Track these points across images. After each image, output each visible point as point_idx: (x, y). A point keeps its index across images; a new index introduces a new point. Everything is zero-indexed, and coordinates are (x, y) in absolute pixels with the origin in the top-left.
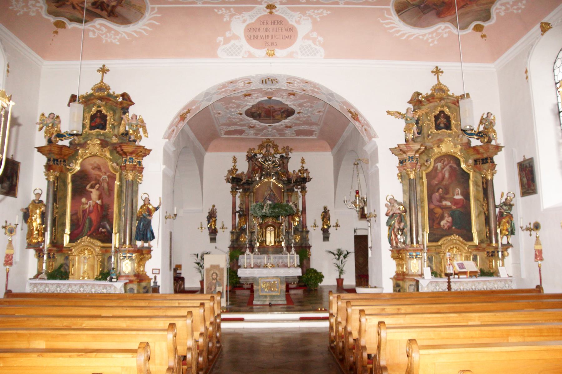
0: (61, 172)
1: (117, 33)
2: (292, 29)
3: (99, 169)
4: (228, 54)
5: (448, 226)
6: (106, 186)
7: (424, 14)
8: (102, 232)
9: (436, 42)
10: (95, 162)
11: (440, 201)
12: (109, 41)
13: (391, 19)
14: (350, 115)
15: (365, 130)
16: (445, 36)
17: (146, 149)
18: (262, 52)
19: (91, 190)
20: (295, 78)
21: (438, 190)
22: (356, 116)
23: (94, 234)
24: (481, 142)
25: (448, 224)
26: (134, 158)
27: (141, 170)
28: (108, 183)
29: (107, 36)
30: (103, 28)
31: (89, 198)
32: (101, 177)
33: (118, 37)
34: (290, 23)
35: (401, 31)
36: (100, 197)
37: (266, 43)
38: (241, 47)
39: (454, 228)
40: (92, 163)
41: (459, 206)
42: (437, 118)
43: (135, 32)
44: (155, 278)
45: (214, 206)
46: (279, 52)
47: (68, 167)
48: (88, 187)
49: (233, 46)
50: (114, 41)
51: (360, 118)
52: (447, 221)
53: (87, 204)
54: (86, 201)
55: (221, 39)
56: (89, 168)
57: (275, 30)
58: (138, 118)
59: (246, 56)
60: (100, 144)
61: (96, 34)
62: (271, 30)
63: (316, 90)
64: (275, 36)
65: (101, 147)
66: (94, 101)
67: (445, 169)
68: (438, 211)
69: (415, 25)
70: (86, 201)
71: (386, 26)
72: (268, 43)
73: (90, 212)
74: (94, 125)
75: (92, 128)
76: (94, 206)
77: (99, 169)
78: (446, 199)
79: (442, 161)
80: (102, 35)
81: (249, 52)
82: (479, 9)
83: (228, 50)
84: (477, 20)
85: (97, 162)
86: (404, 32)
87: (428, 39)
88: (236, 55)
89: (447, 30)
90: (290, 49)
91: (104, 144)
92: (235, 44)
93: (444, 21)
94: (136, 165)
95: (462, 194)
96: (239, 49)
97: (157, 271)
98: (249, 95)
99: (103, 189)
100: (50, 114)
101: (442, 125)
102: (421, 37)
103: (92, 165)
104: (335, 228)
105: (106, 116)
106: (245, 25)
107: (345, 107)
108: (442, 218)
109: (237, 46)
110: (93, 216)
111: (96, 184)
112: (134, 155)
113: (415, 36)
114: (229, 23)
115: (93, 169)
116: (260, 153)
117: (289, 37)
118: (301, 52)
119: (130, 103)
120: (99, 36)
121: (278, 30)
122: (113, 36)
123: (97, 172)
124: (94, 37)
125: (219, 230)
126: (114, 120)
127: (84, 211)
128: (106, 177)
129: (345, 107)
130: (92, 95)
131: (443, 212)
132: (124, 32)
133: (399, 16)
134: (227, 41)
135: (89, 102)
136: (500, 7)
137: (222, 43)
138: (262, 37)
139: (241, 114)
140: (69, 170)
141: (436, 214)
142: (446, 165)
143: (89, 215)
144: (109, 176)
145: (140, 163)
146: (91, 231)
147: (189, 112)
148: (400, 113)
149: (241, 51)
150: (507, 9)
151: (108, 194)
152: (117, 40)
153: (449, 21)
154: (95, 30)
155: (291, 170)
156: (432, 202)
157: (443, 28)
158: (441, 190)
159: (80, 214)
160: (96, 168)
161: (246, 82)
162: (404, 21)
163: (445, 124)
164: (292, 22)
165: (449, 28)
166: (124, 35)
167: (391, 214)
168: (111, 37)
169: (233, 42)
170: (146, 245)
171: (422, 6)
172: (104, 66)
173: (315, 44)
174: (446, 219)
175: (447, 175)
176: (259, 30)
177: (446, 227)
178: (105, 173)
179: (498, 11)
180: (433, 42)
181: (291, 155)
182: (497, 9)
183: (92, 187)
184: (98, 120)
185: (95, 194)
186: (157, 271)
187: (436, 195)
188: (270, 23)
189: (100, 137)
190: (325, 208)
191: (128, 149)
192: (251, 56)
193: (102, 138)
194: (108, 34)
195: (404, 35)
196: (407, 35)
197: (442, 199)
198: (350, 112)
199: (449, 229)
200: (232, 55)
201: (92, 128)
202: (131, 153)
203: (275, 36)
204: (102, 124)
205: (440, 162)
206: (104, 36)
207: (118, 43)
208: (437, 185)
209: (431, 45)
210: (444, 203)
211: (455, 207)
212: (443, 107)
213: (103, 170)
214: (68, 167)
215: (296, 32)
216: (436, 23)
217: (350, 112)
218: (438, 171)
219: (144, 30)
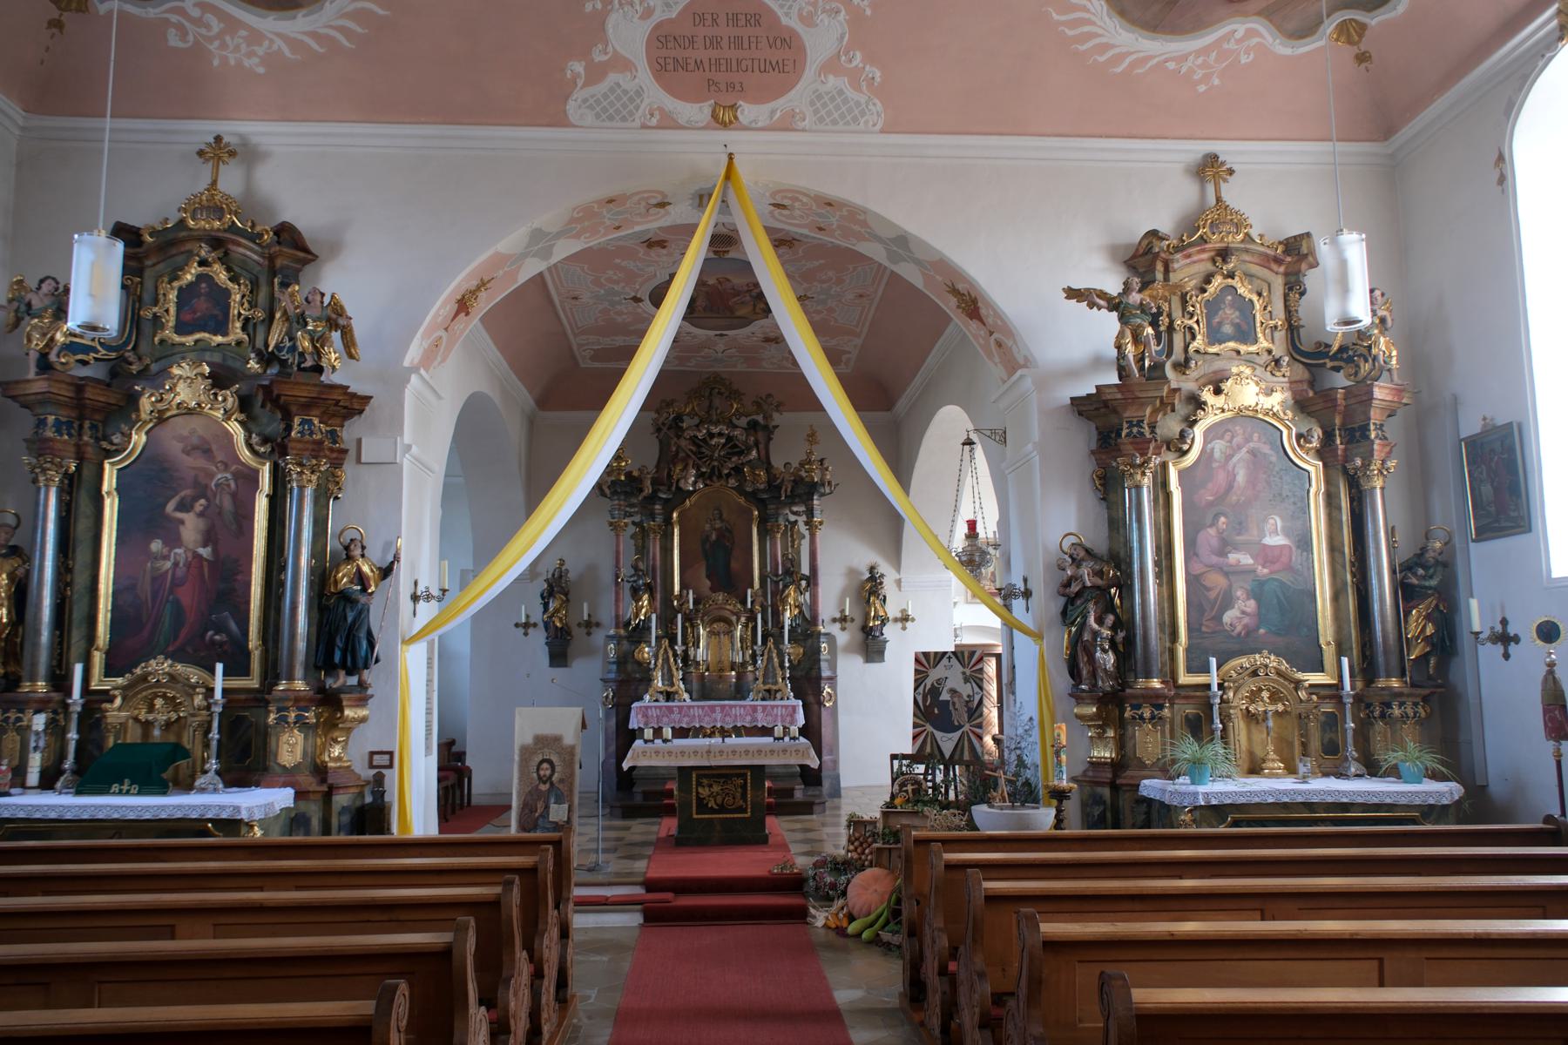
0: (80, 458)
1: (256, 37)
2: (788, 42)
3: (207, 452)
4: (598, 116)
5: (1246, 626)
6: (227, 503)
8: (213, 642)
9: (1216, 82)
10: (193, 431)
11: (1222, 553)
12: (232, 62)
14: (953, 301)
15: (999, 345)
17: (354, 395)
18: (699, 112)
19: (179, 515)
20: (796, 194)
21: (1216, 517)
22: (972, 305)
23: (190, 650)
24: (1348, 376)
25: (1246, 620)
26: (316, 421)
27: (338, 457)
28: (234, 496)
29: (223, 46)
30: (209, 17)
31: (173, 540)
32: (212, 476)
33: (260, 51)
34: (784, 21)
36: (209, 538)
37: (711, 83)
38: (639, 93)
39: (1262, 631)
40: (185, 433)
41: (1277, 567)
42: (1212, 307)
43: (314, 35)
44: (379, 780)
45: (562, 562)
46: (748, 112)
47: (105, 444)
48: (170, 507)
49: (612, 90)
50: (247, 63)
51: (983, 312)
52: (1243, 612)
53: (166, 558)
54: (165, 551)
55: (578, 67)
56: (174, 448)
57: (737, 42)
58: (327, 300)
59: (654, 121)
60: (211, 376)
61: (191, 38)
62: (725, 43)
63: (857, 228)
64: (739, 62)
65: (213, 386)
66: (188, 246)
67: (1235, 459)
68: (1216, 581)
70: (165, 551)
71: (1070, 33)
72: (716, 84)
73: (176, 583)
74: (187, 317)
75: (181, 329)
76: (188, 565)
77: (207, 452)
78: (1237, 548)
79: (1228, 436)
80: (211, 40)
81: (661, 109)
83: (598, 102)
84: (1347, 7)
85: (200, 431)
86: (1124, 50)
87: (1191, 71)
88: (624, 119)
89: (1256, 40)
90: (781, 104)
91: (219, 380)
92: (618, 85)
93: (1245, 14)
94: (320, 443)
95: (1287, 534)
96: (631, 100)
97: (385, 760)
98: (662, 244)
99: (220, 514)
100: (42, 281)
101: (1228, 329)
102: (1171, 65)
103: (181, 439)
104: (899, 625)
105: (227, 293)
106: (646, 27)
107: (939, 278)
108: (1227, 602)
109: (625, 92)
110: (188, 597)
111: (195, 499)
112: (317, 412)
113: (1155, 61)
114: (600, 20)
115: (188, 453)
116: (692, 414)
117: (779, 67)
118: (816, 112)
119: (301, 255)
120: (197, 43)
121: (746, 45)
122: (244, 46)
123: (200, 462)
124: (181, 45)
125: (578, 633)
126: (253, 305)
127: (158, 578)
128: (229, 476)
129: (939, 278)
130: (181, 223)
131: (1230, 586)
132: (278, 35)
134: (596, 73)
135: (174, 251)
137: (580, 83)
138: (699, 65)
139: (637, 300)
140: (109, 454)
141: (1208, 589)
142: (1239, 448)
143: (171, 591)
144: (236, 476)
145: (334, 436)
146: (178, 643)
147: (483, 284)
148: (1102, 295)
149: (637, 108)
151: (234, 527)
152: (256, 60)
153: (1259, 14)
154: (187, 24)
155: (777, 462)
156: (1196, 554)
157: (1238, 35)
158: (1223, 519)
159: (145, 589)
160: (195, 448)
161: (654, 201)
163: (1237, 326)
164: (790, 21)
165: (1260, 35)
166: (279, 43)
167: (1075, 588)
168: (237, 48)
169: (612, 77)
170: (353, 680)
172: (218, 139)
173: (856, 85)
174: (1240, 604)
175: (1241, 477)
176: (692, 41)
177: (1239, 628)
178: (226, 466)
180: (1206, 78)
181: (777, 418)
183: (184, 507)
184: (202, 305)
185: (191, 527)
186: (385, 760)
187: (1209, 536)
188: (722, 20)
189: (208, 356)
190: (872, 569)
191: (299, 391)
192: (668, 122)
193: (217, 358)
194: (228, 38)
195: (1120, 57)
197: (1225, 546)
198: (955, 291)
199: (1248, 634)
200: (611, 118)
201: (181, 329)
202: (307, 406)
203: (739, 62)
204: (216, 316)
205: (1222, 438)
206: (217, 43)
207: (261, 70)
208: (1211, 504)
209: (1202, 88)
210: (1233, 557)
211: (1266, 571)
212: (1231, 275)
213: (220, 456)
214: (105, 444)
215: (802, 49)
216: (1220, 20)
217: (955, 291)
218: (1215, 465)
219: (341, 29)
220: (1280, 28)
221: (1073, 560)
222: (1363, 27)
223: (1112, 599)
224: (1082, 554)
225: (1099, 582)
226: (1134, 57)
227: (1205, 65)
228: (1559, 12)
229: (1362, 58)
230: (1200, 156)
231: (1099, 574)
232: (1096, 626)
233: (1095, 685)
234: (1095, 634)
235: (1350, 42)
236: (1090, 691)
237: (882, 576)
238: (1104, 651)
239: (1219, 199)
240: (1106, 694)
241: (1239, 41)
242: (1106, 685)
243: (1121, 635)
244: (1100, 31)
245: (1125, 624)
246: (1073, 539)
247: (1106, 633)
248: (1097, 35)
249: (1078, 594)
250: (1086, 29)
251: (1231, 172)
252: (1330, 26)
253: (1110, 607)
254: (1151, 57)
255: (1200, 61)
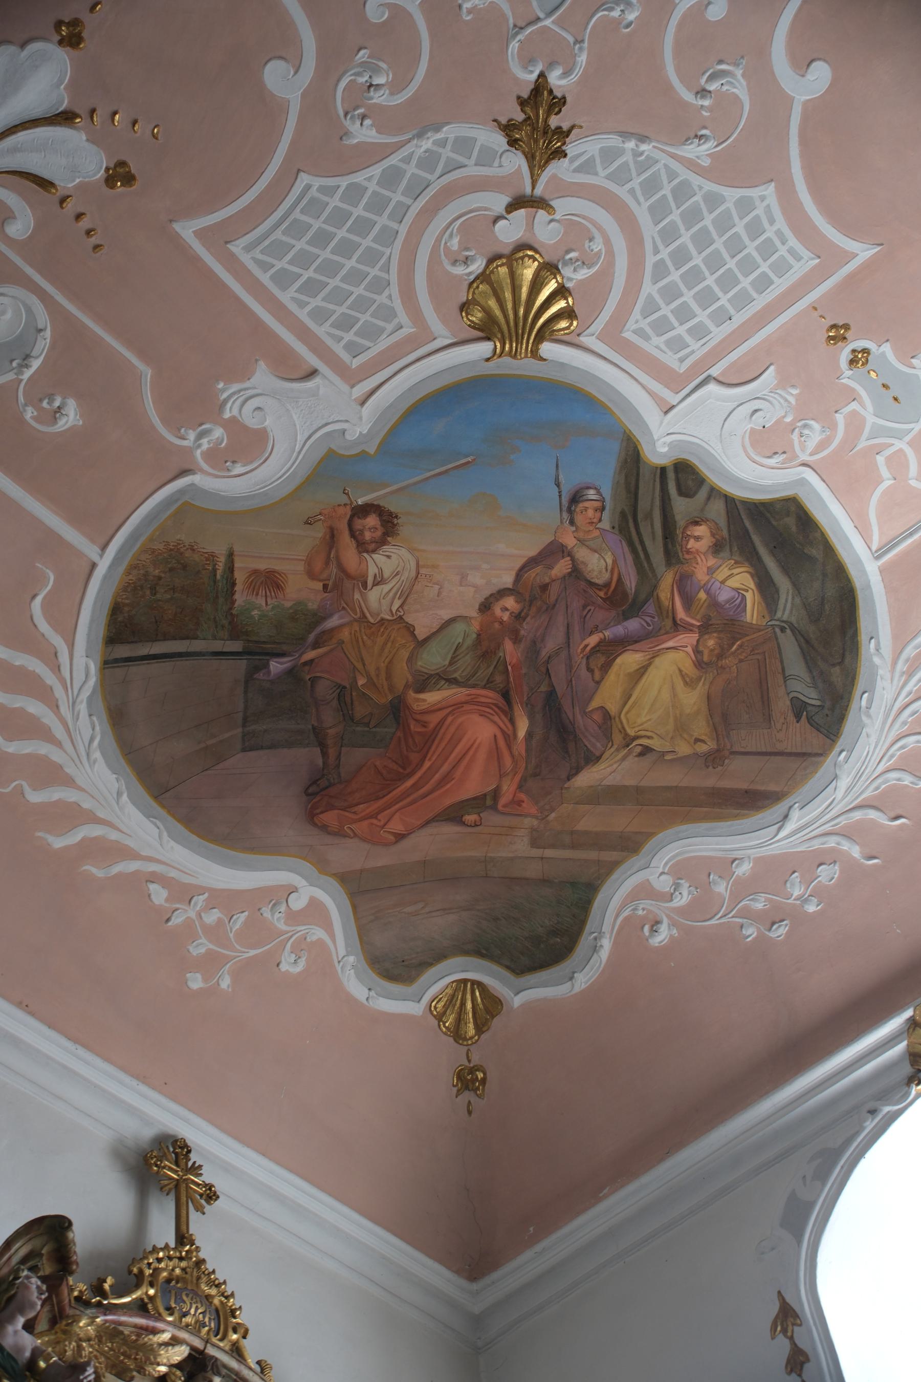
7: (250, 744)
9: (225, 983)
13: (51, 659)
16: (290, 965)
35: (69, 782)
69: (165, 786)
82: (533, 871)
87: (189, 931)
89: (318, 933)
93: (322, 865)
113: (132, 866)
133: (107, 664)
136: (664, 883)
150: (703, 905)
153: (343, 878)
157: (298, 902)
162: (118, 717)
165: (328, 927)
171: (276, 666)
179: (644, 906)
182: (645, 891)
195: (72, 815)
196: (95, 831)
209: (196, 982)
220: (363, 932)
222: (492, 1005)
226: (95, 831)
227: (216, 932)
228: (913, 1024)
229: (468, 1080)
230: (148, 1133)
235: (457, 1034)
239: (183, 1238)
241: (294, 917)
244: (59, 732)
248: (47, 735)
250: (34, 707)
251: (211, 1195)
252: (439, 981)
254: (134, 856)
255: (212, 917)
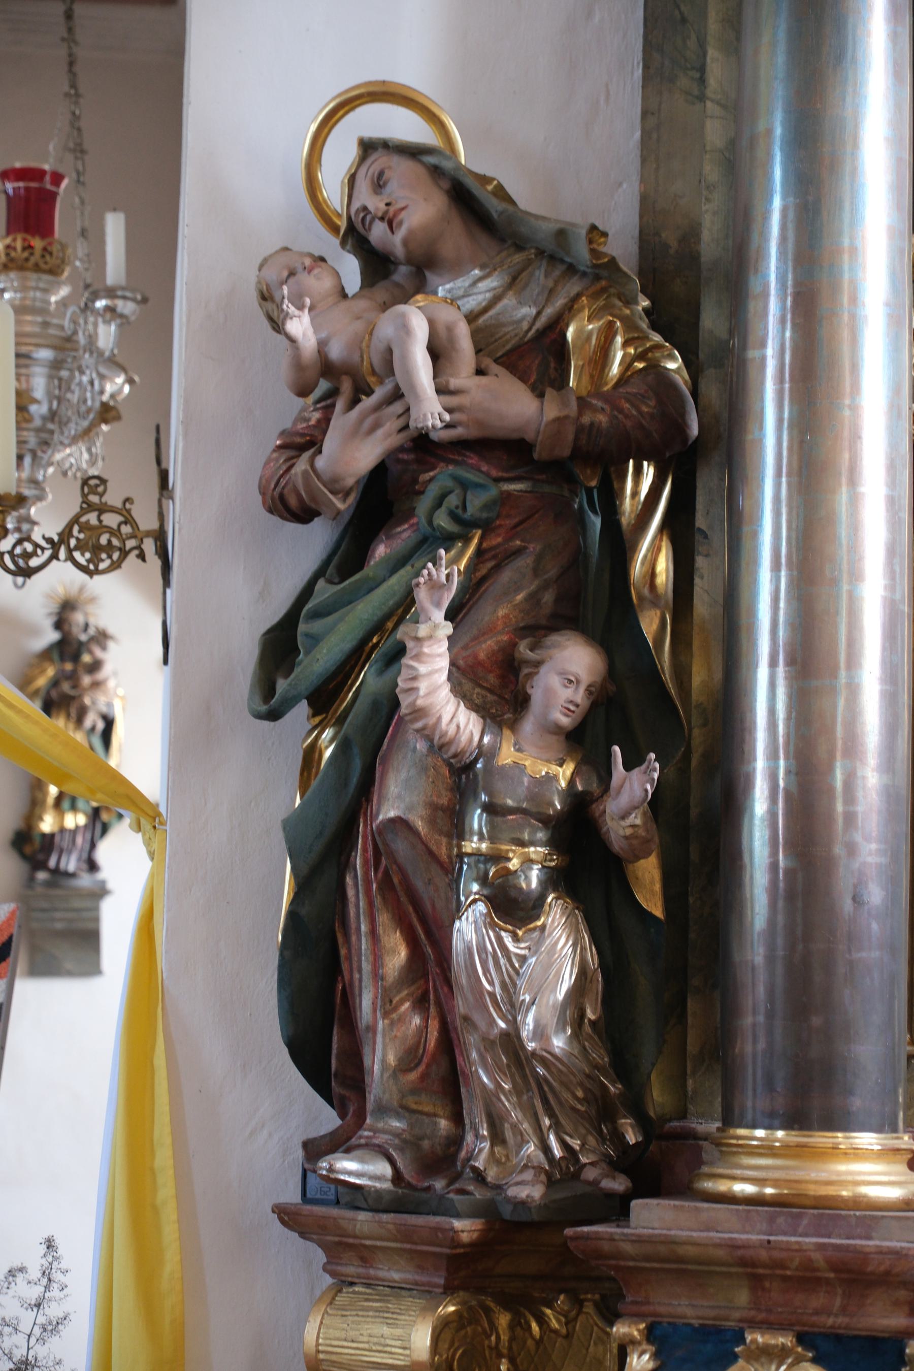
167: (354, 451)
221: (376, 265)
223: (619, 545)
224: (420, 209)
225: (514, 405)
231: (539, 357)
232: (461, 723)
233: (445, 1159)
234: (462, 775)
236: (403, 1199)
237: (102, 638)
238: (512, 908)
240: (507, 1228)
242: (520, 1157)
243: (632, 788)
245: (666, 713)
246: (403, 126)
247: (538, 767)
249: (380, 501)
253: (594, 599)
